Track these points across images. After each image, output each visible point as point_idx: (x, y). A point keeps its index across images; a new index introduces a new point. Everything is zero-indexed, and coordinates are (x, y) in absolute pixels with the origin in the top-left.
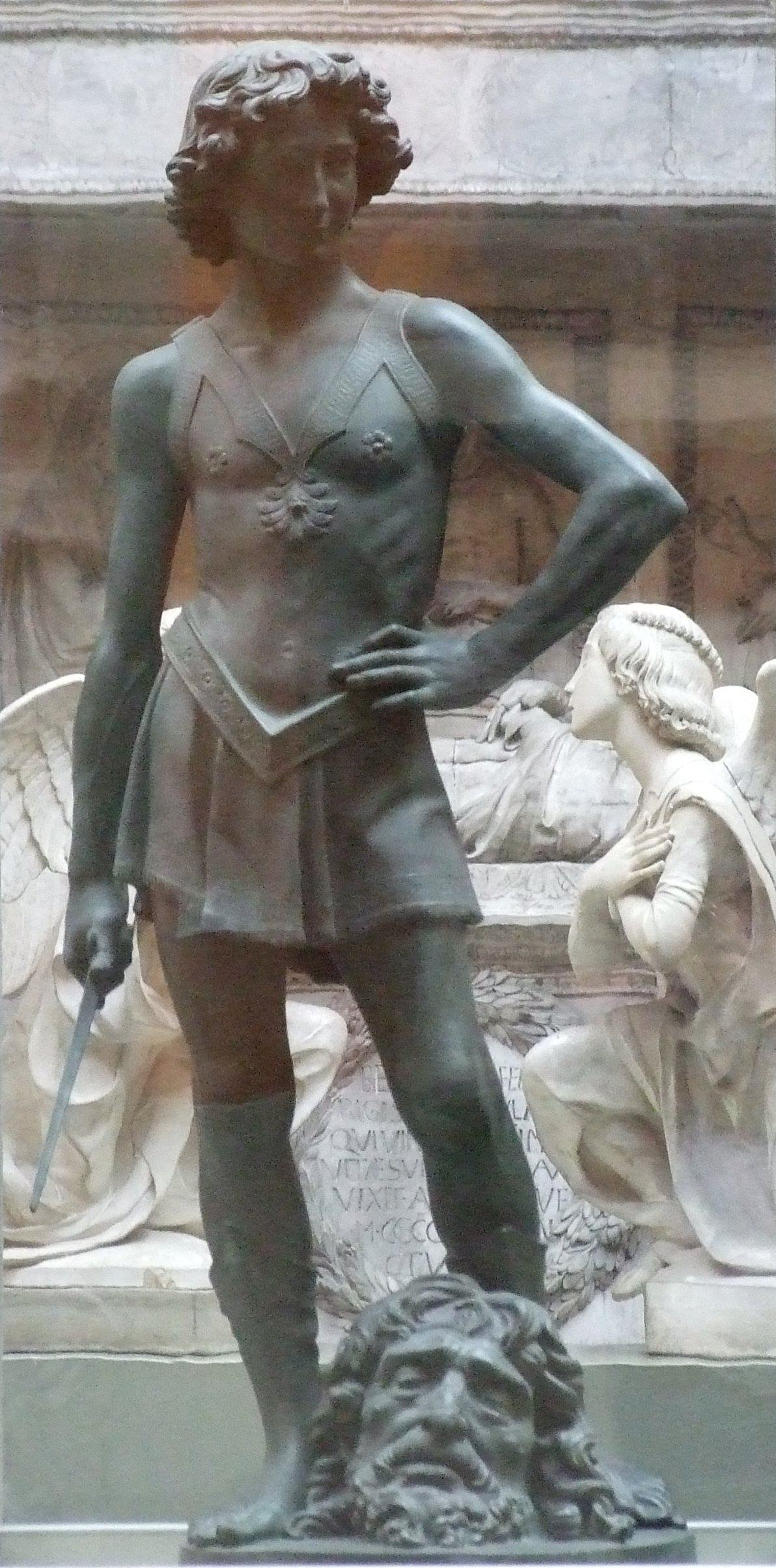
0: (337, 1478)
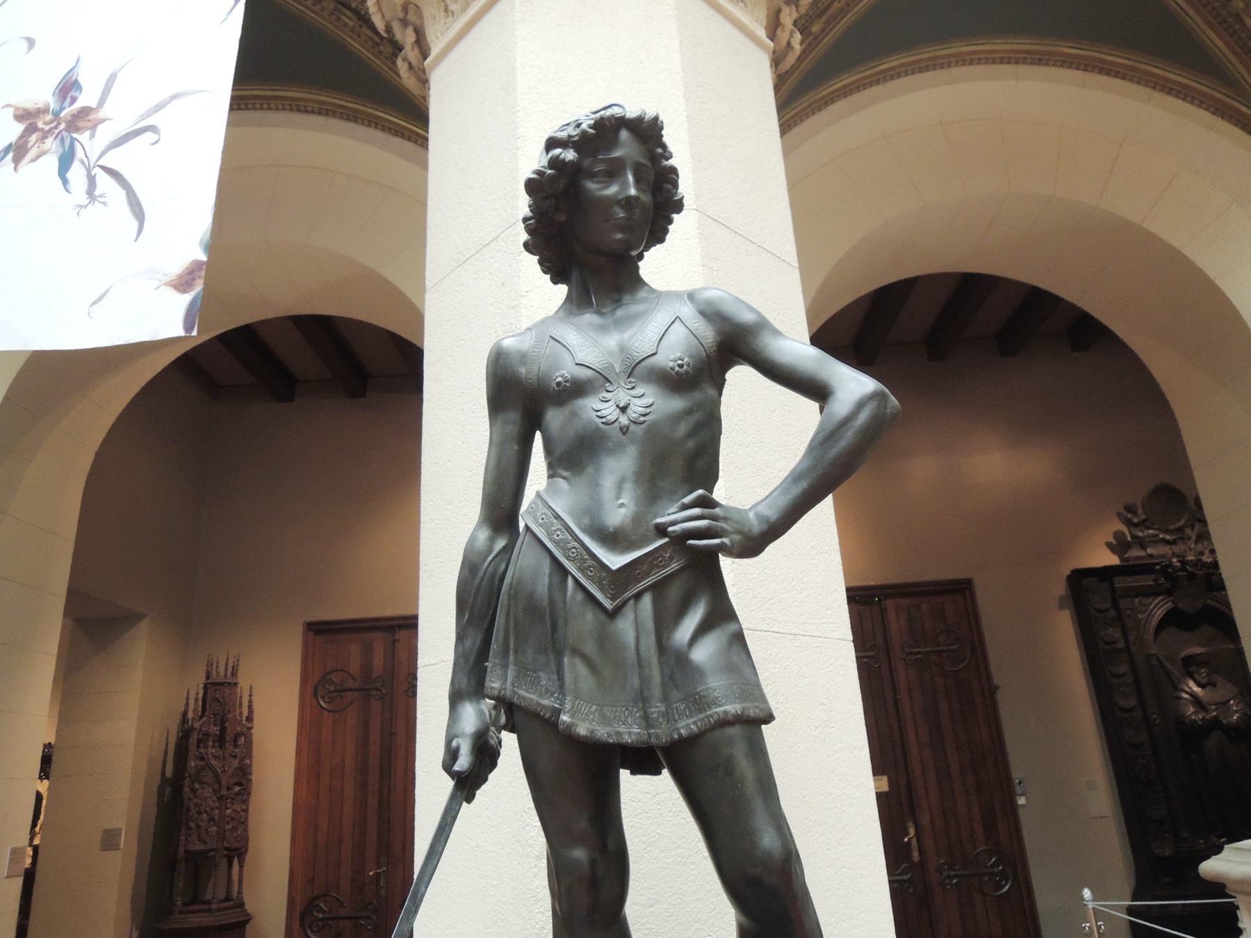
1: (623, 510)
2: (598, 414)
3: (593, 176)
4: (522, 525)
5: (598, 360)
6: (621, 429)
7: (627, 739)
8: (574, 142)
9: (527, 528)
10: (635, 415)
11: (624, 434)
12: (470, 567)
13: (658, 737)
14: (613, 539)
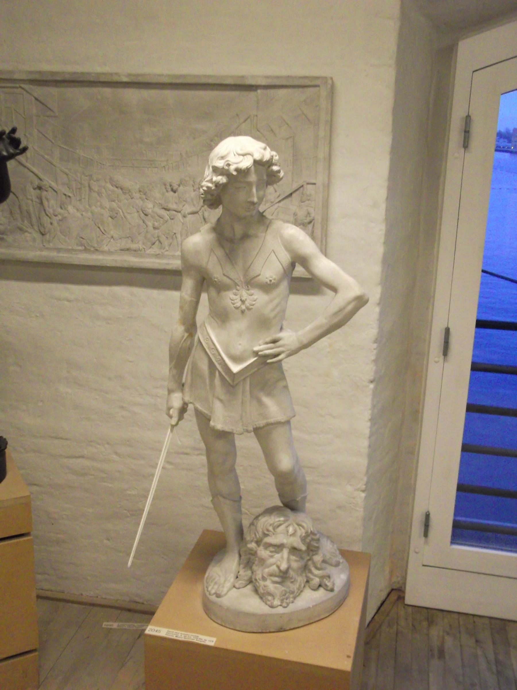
2: (233, 302)
4: (196, 338)
9: (200, 341)
14: (236, 359)
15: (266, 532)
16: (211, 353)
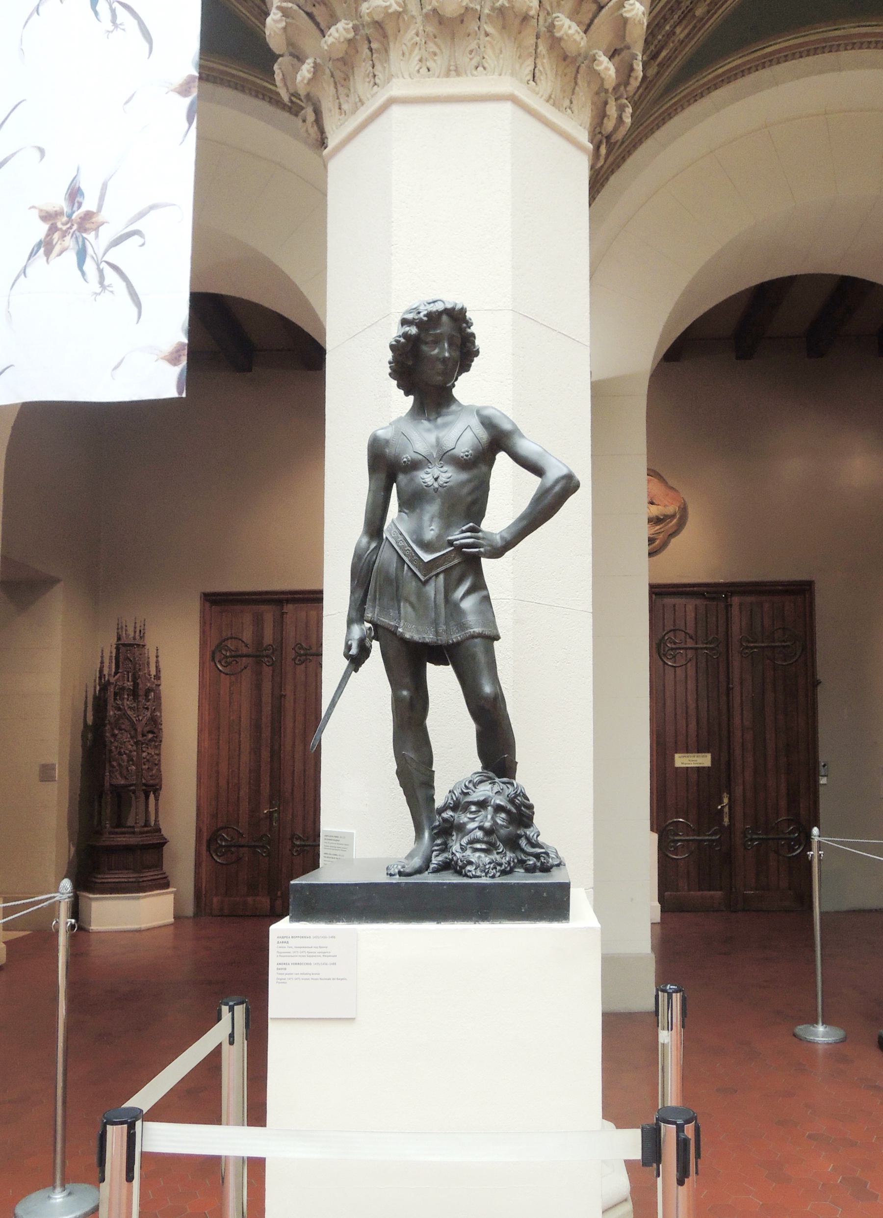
0: (445, 848)
1: (432, 532)
3: (426, 343)
5: (425, 450)
6: (434, 490)
7: (427, 640)
8: (416, 323)
9: (387, 538)
10: (441, 483)
11: (436, 492)
12: (358, 557)
13: (441, 640)
14: (427, 547)
15: (465, 791)
16: (398, 546)
